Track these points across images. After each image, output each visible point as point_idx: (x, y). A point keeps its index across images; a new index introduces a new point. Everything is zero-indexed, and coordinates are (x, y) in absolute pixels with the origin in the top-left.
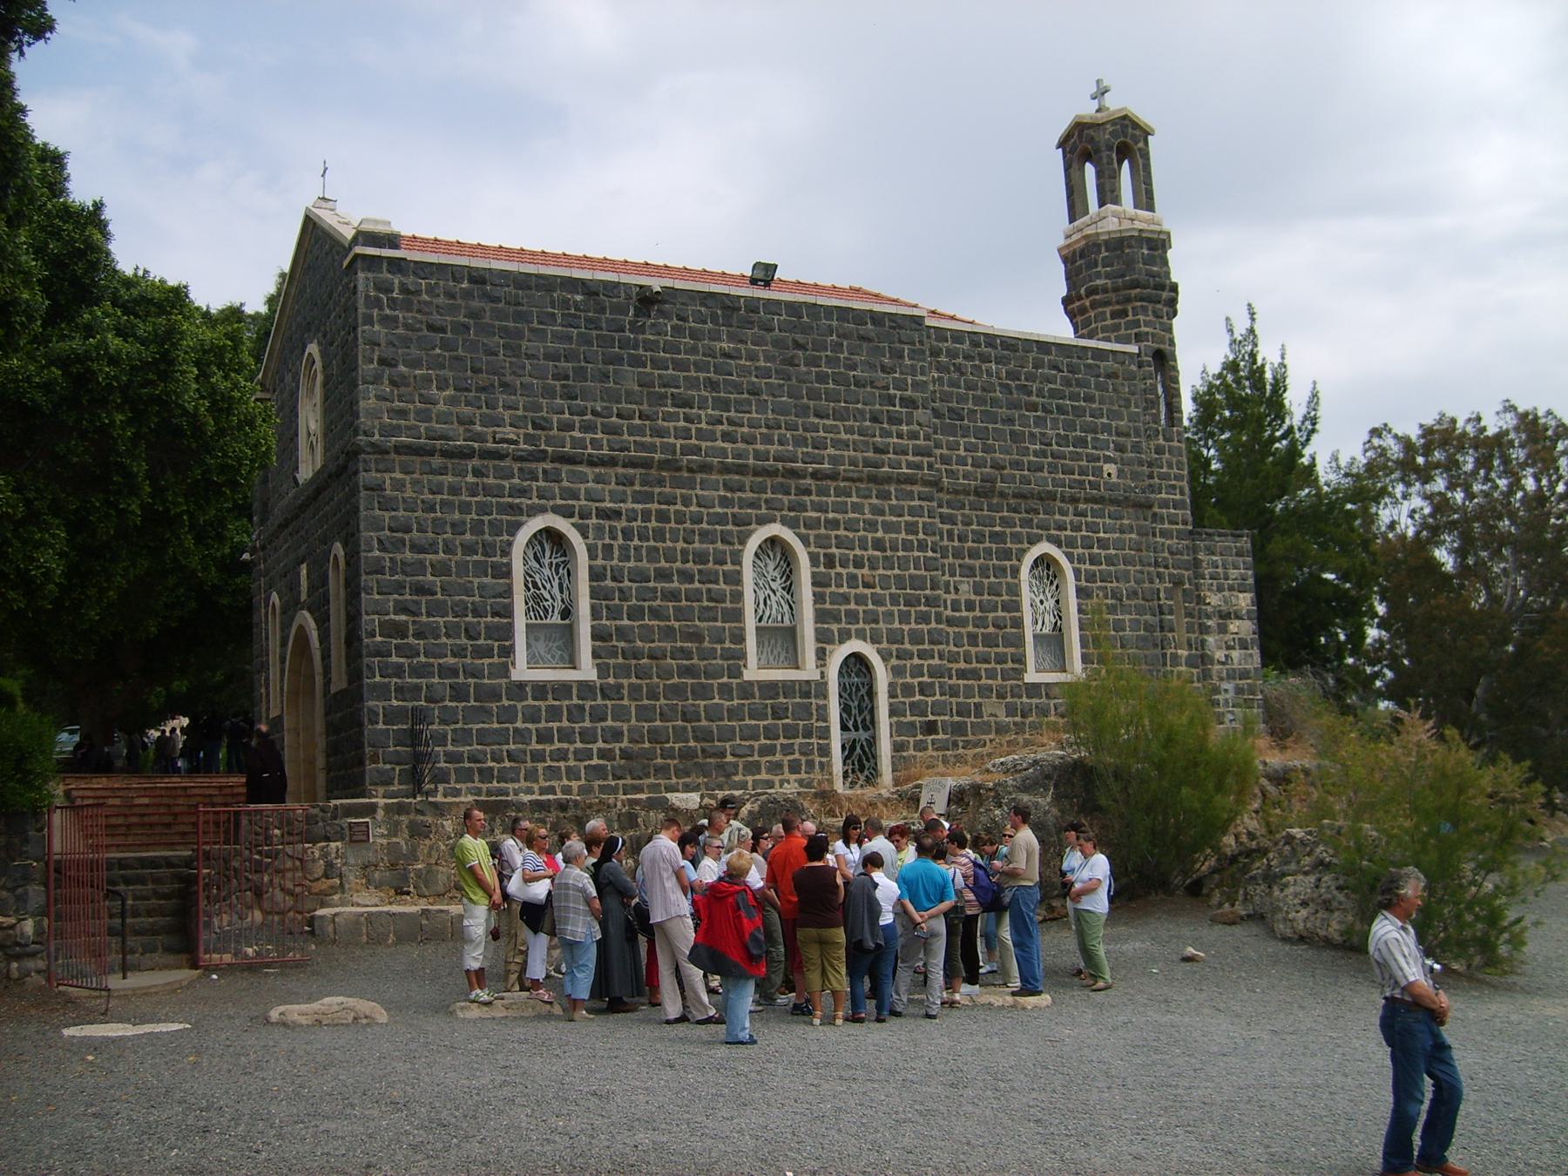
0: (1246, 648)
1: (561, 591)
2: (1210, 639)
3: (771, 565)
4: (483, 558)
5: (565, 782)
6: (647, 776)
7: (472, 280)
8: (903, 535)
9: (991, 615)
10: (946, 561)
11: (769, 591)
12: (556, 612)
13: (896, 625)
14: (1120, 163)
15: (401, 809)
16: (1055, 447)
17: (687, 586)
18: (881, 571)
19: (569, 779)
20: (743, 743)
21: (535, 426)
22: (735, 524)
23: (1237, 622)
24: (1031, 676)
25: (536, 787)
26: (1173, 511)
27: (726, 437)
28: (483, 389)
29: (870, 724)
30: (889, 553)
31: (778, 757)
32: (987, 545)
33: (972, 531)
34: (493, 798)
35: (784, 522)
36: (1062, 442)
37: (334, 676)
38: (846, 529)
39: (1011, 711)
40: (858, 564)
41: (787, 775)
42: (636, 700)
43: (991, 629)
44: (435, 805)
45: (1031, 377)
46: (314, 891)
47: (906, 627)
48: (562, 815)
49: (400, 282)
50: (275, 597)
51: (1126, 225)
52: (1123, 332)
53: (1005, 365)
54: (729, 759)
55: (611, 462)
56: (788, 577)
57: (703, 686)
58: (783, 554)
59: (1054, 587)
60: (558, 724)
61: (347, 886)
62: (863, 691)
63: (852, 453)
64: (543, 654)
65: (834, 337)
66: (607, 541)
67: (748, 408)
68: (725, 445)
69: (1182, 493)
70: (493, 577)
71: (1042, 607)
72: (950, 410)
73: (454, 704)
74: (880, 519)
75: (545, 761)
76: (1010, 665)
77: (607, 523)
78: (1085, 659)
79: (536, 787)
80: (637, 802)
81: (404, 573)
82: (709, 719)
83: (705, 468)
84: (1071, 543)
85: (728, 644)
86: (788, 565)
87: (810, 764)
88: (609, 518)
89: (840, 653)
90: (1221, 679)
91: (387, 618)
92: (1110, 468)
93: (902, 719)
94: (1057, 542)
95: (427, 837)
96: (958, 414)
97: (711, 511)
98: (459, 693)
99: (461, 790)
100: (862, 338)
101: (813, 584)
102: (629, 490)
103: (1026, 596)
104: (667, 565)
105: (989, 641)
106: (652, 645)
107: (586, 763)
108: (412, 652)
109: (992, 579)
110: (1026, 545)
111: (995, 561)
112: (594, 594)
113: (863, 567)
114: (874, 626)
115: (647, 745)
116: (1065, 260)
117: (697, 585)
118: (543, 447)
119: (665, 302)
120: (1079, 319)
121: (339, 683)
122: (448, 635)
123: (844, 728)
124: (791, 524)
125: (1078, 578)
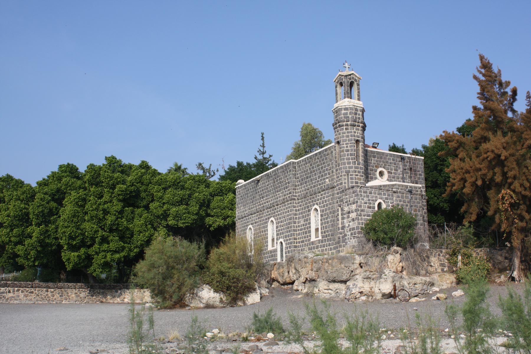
23: (352, 214)
45: (314, 164)
78: (322, 233)
89: (279, 242)
90: (347, 232)
92: (327, 180)
124: (274, 217)
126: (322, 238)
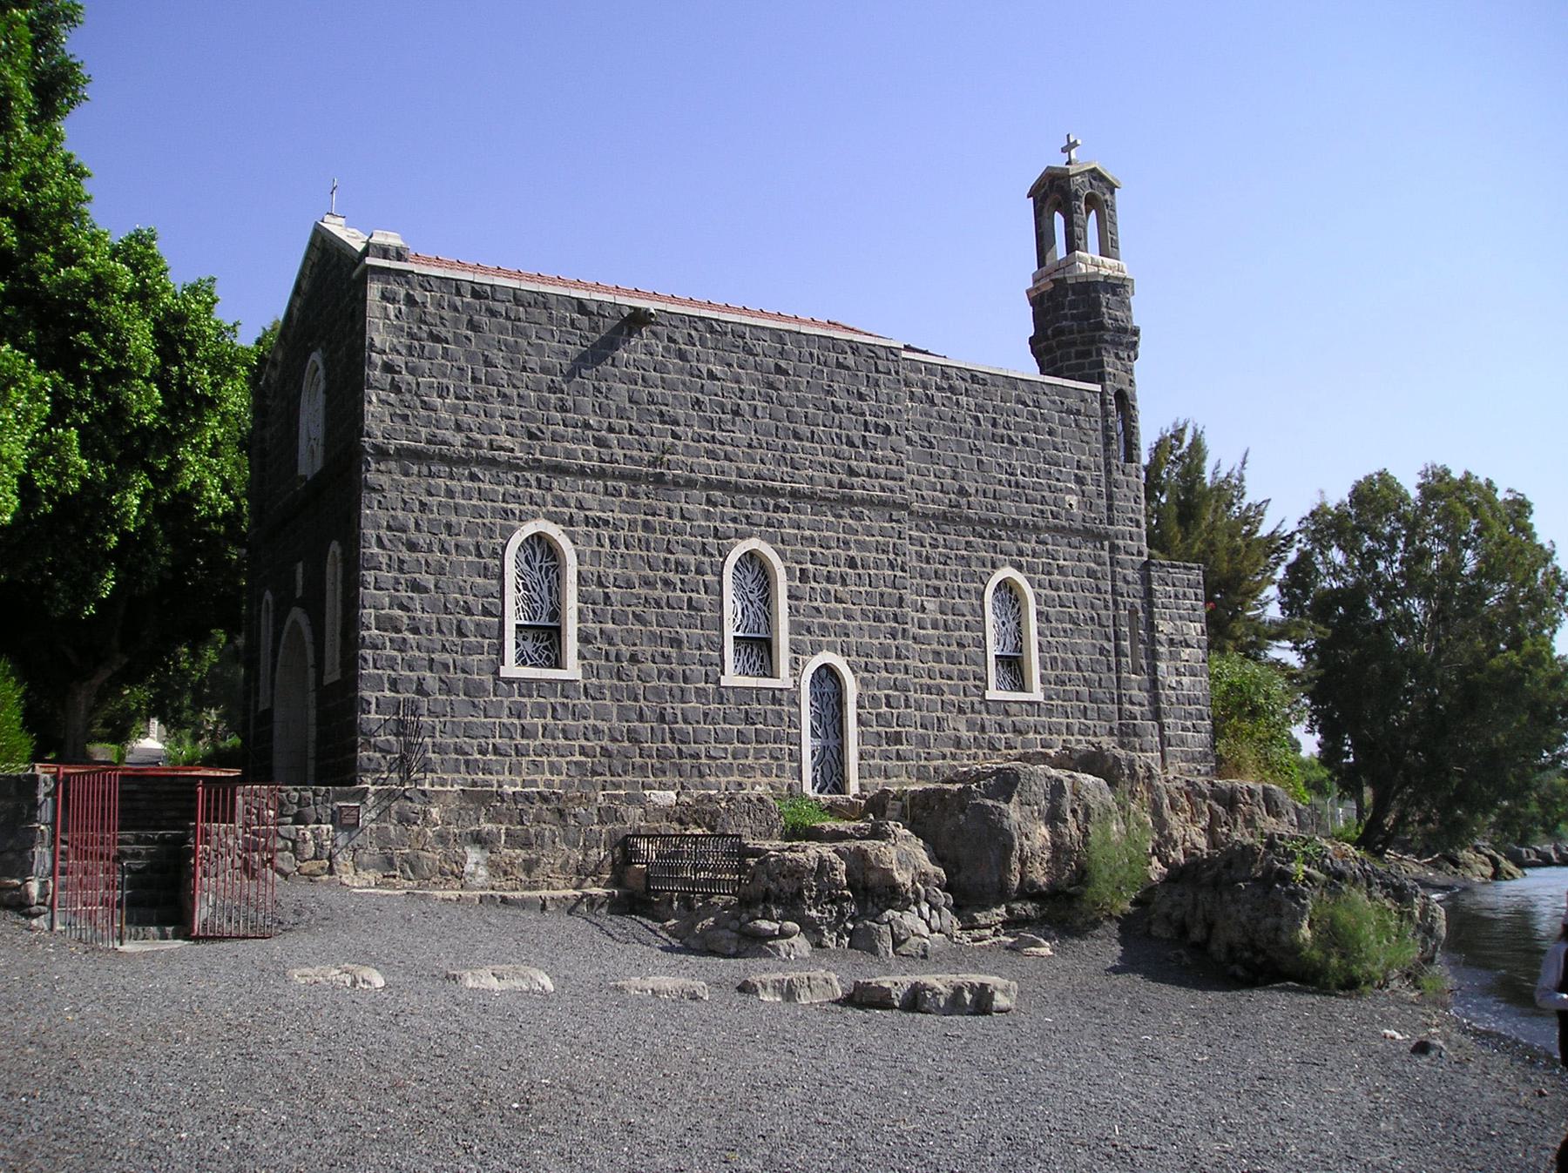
0: (1196, 676)
1: (550, 595)
2: (1162, 666)
3: (750, 578)
4: (477, 559)
5: (548, 776)
6: (626, 772)
7: (476, 294)
8: (874, 554)
9: (957, 634)
10: (914, 581)
11: (747, 602)
12: (545, 613)
13: (867, 639)
14: (1088, 213)
15: (391, 795)
16: (1020, 478)
17: (670, 594)
18: (854, 588)
19: (552, 774)
20: (718, 745)
21: (531, 436)
22: (716, 536)
23: (1188, 650)
24: (992, 694)
25: (519, 780)
26: (1130, 542)
27: (712, 455)
28: (484, 399)
29: (840, 732)
30: (861, 571)
31: (750, 761)
32: (954, 567)
33: (940, 554)
34: (479, 788)
35: (761, 536)
36: (1026, 473)
37: (328, 668)
38: (822, 546)
39: (971, 725)
40: (829, 579)
41: (759, 778)
42: (618, 700)
43: (954, 648)
44: (424, 793)
46: (303, 871)
47: (876, 642)
48: (545, 807)
49: (408, 294)
50: (268, 596)
51: (1092, 269)
52: (1087, 371)
53: (973, 397)
54: (704, 761)
55: (601, 474)
56: (765, 590)
57: (682, 690)
58: (761, 567)
59: (1016, 610)
60: (543, 721)
61: (335, 867)
62: (833, 701)
63: (829, 475)
64: (530, 653)
65: (815, 364)
66: (596, 548)
67: (733, 428)
68: (710, 462)
69: (1138, 525)
70: (485, 577)
71: (1004, 629)
72: (925, 439)
73: (445, 697)
74: (853, 538)
75: (529, 755)
76: (971, 682)
77: (594, 531)
78: (1043, 679)
79: (519, 780)
80: (616, 797)
81: (401, 570)
82: (686, 721)
83: (691, 484)
84: (1031, 569)
85: (705, 651)
86: (766, 578)
87: (781, 768)
88: (598, 526)
91: (383, 612)
93: (869, 728)
94: (1019, 567)
95: (415, 823)
96: (930, 443)
97: (694, 523)
98: (447, 686)
99: (447, 780)
100: (839, 365)
101: (789, 597)
102: (617, 500)
103: (990, 618)
104: (651, 573)
105: (952, 660)
106: (635, 648)
107: (568, 759)
108: (402, 646)
109: (958, 600)
110: (989, 570)
111: (960, 583)
112: (582, 598)
113: (835, 583)
114: (845, 639)
115: (626, 744)
116: (1034, 302)
117: (679, 593)
118: (538, 456)
119: (658, 324)
120: (1046, 358)
121: (332, 675)
122: (440, 631)
123: (814, 734)
124: (771, 540)
125: (1038, 603)
126: (1048, 698)
